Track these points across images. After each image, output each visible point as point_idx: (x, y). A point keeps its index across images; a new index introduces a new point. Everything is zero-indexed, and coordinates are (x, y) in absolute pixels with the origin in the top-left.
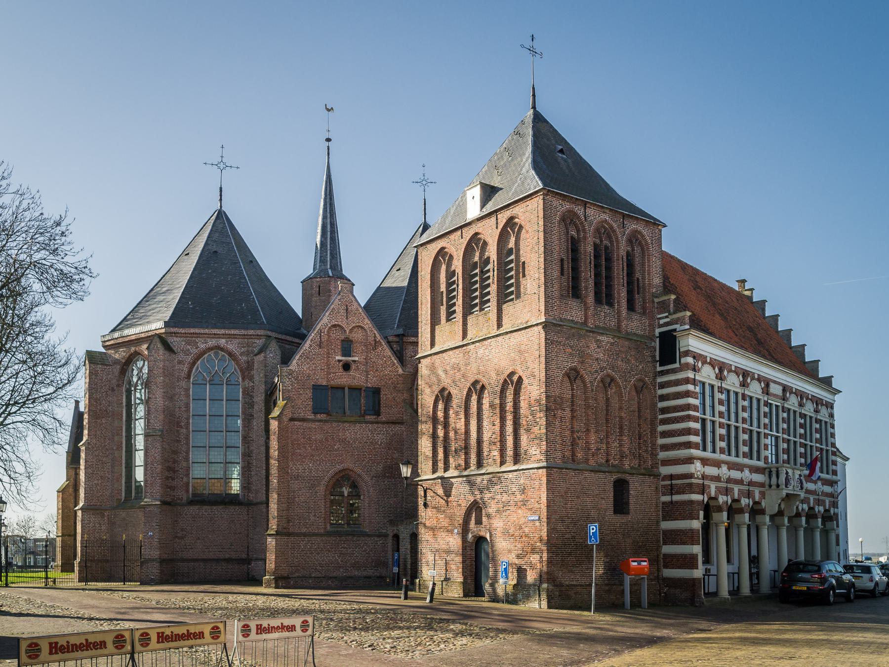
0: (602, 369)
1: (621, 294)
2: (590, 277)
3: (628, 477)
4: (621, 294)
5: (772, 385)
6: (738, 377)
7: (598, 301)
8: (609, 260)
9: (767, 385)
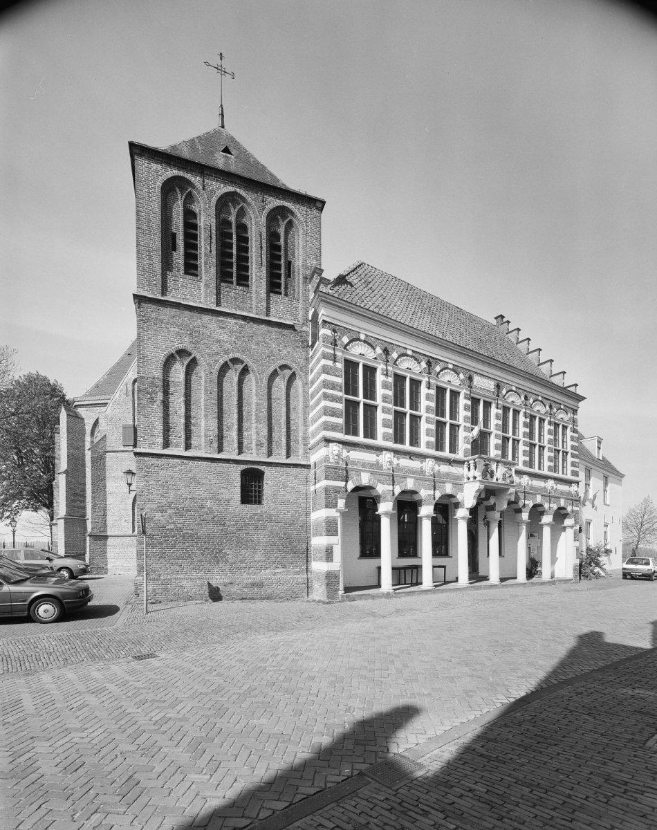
0: (227, 352)
1: (258, 273)
2: (211, 252)
3: (262, 468)
4: (258, 273)
5: (476, 379)
6: (419, 363)
7: (223, 275)
8: (243, 240)
9: (470, 379)
